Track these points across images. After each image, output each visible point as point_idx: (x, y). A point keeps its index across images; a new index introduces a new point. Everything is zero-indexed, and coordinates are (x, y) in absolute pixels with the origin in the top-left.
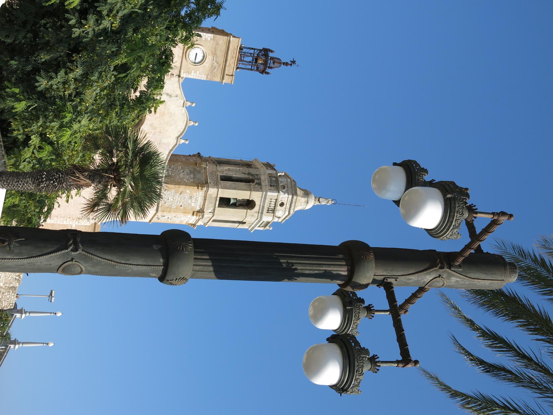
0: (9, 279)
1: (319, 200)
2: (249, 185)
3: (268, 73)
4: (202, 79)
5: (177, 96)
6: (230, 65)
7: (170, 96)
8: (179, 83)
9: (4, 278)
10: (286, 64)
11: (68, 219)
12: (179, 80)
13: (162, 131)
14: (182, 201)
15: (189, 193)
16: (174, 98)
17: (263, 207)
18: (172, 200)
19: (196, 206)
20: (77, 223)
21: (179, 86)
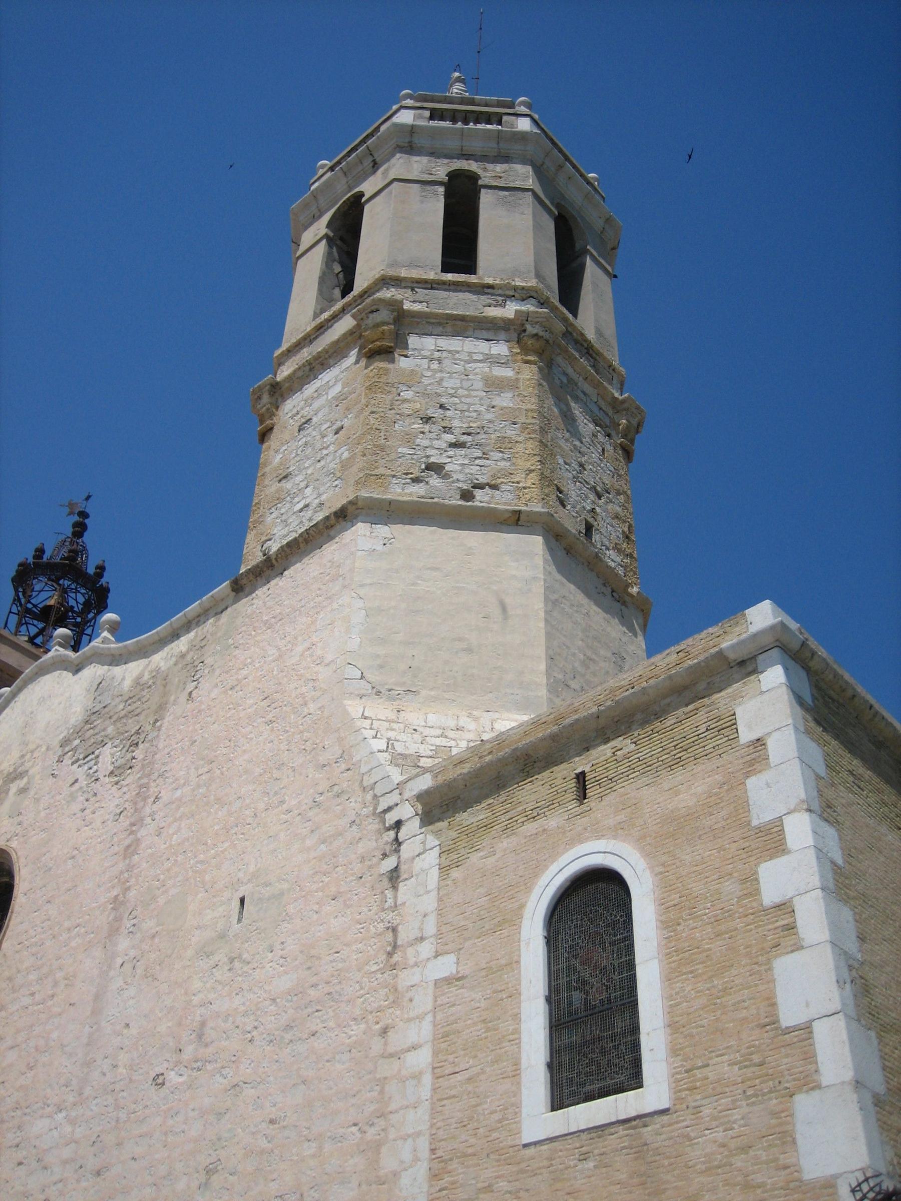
10: (80, 529)
11: (396, 1041)
18: (308, 491)
20: (426, 949)
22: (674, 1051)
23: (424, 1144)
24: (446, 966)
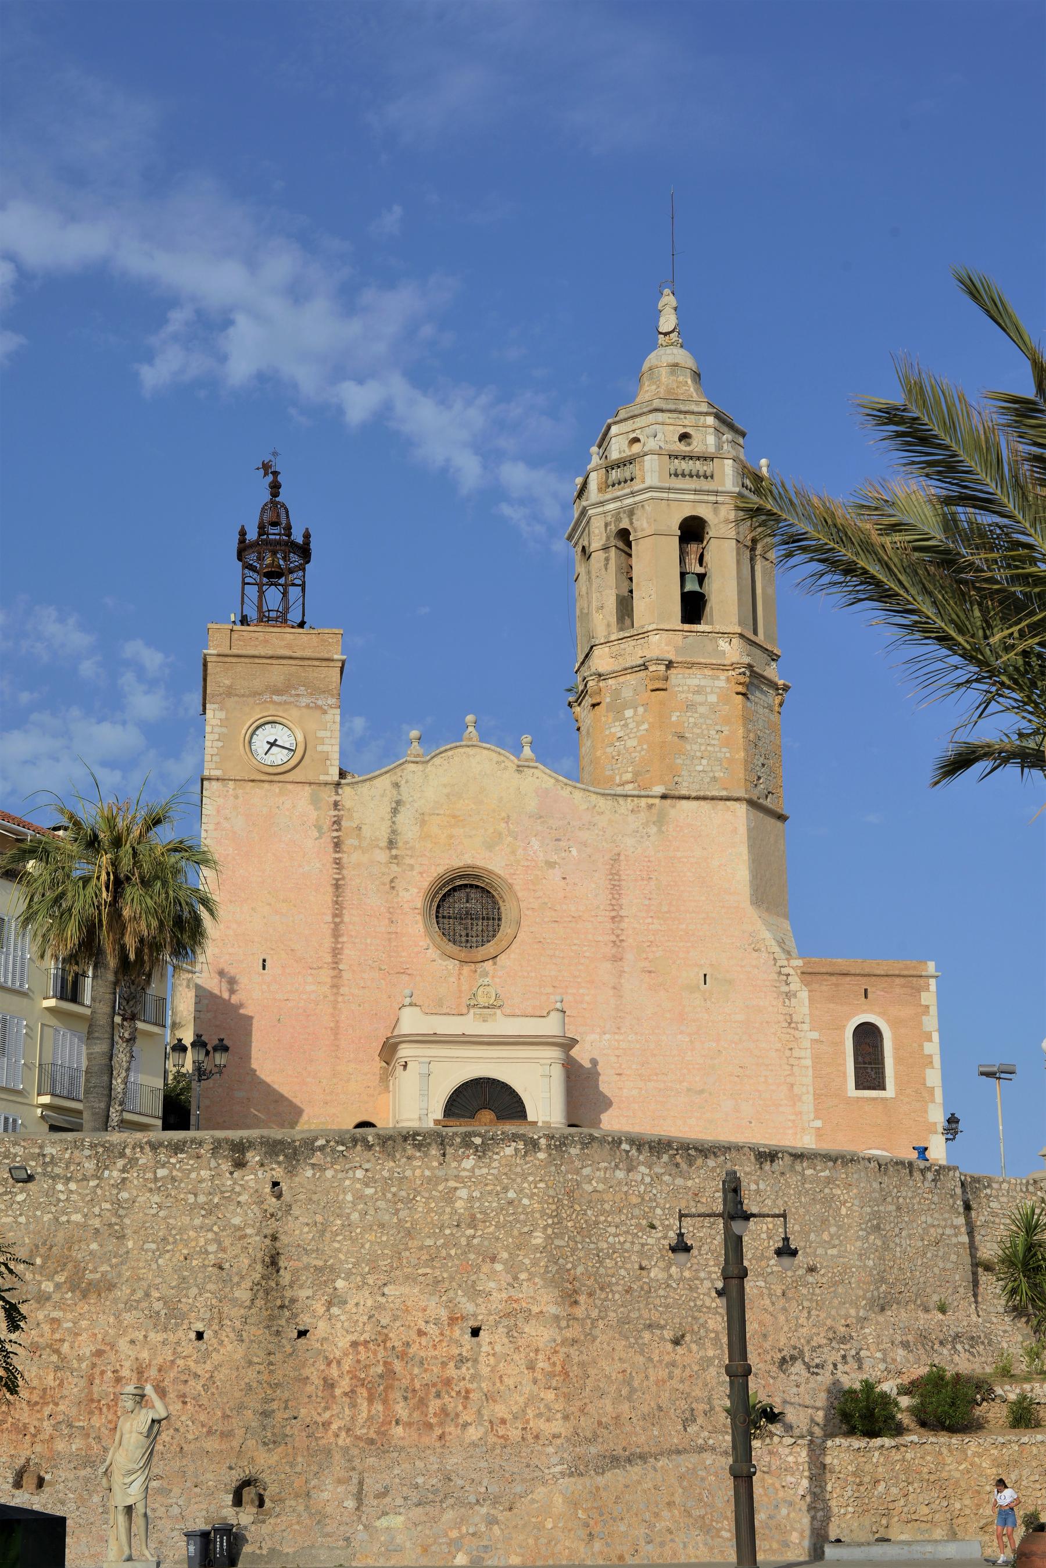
0: (936, 1199)
1: (666, 334)
2: (637, 545)
3: (307, 536)
4: (338, 718)
5: (396, 785)
6: (289, 646)
7: (398, 803)
8: (357, 783)
9: (936, 1215)
10: (275, 488)
12: (348, 784)
13: (504, 814)
14: (706, 732)
15: (678, 714)
16: (404, 788)
17: (696, 491)
18: (704, 762)
19: (718, 690)
20: (806, 1027)
21: (368, 783)
22: (896, 1084)
23: (811, 1089)
24: (815, 1035)
